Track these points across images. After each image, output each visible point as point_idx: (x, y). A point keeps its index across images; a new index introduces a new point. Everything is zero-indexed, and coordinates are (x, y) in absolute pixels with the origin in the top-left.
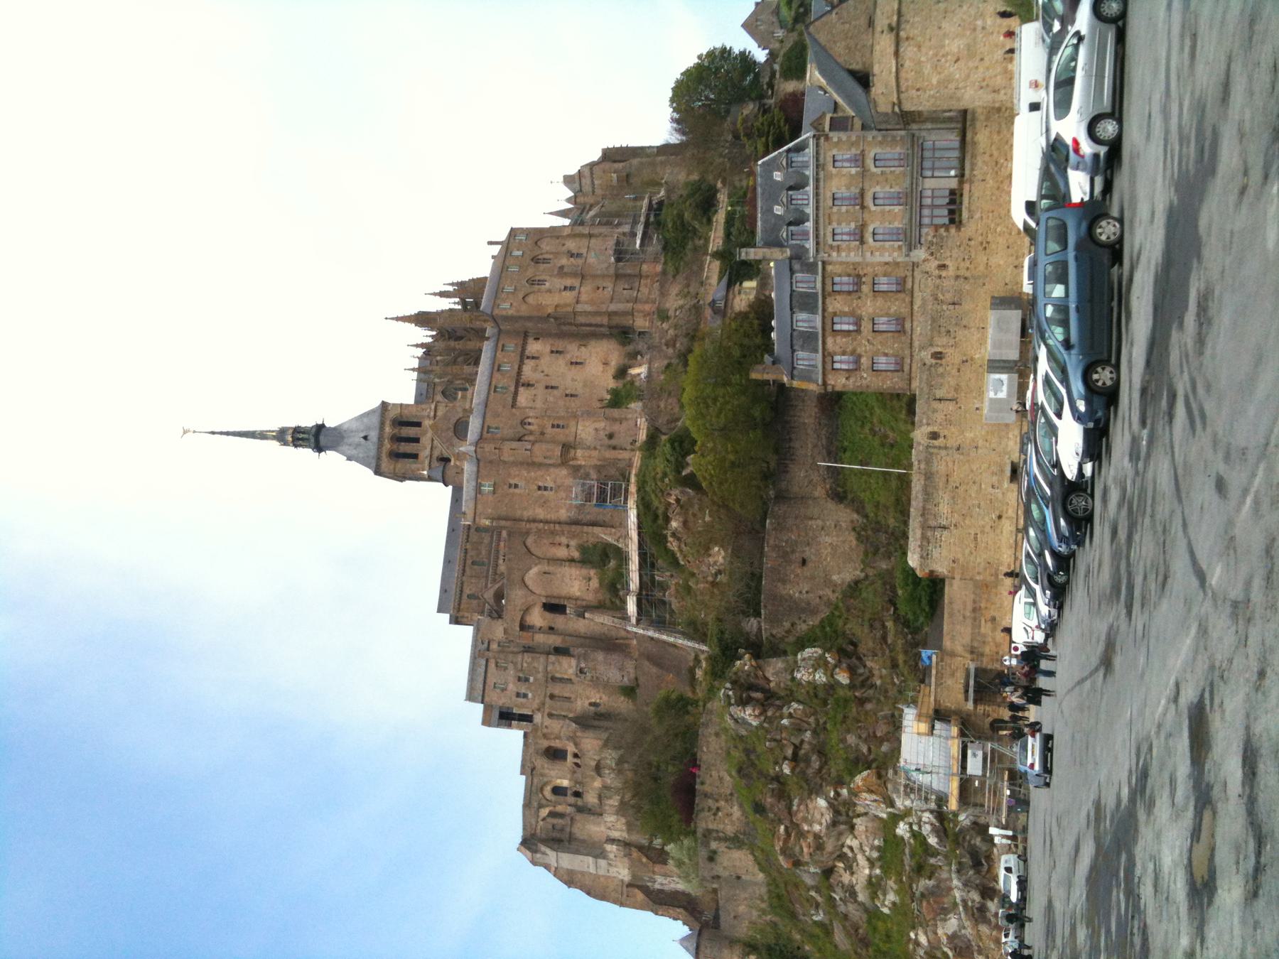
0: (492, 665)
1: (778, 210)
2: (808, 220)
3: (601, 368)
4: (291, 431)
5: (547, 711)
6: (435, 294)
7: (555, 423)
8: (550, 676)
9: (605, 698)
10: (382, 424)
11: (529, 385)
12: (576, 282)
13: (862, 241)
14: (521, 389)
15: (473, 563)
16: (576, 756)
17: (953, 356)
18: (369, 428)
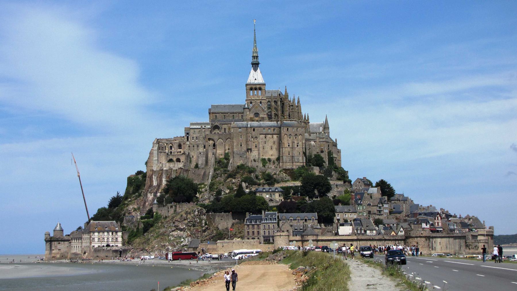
0: (199, 130)
2: (267, 221)
3: (271, 154)
4: (256, 55)
5: (190, 145)
6: (294, 97)
7: (257, 145)
8: (198, 145)
9: (195, 159)
10: (259, 85)
11: (265, 137)
13: (264, 229)
14: (264, 135)
15: (225, 116)
16: (180, 152)
17: (243, 244)
18: (258, 80)
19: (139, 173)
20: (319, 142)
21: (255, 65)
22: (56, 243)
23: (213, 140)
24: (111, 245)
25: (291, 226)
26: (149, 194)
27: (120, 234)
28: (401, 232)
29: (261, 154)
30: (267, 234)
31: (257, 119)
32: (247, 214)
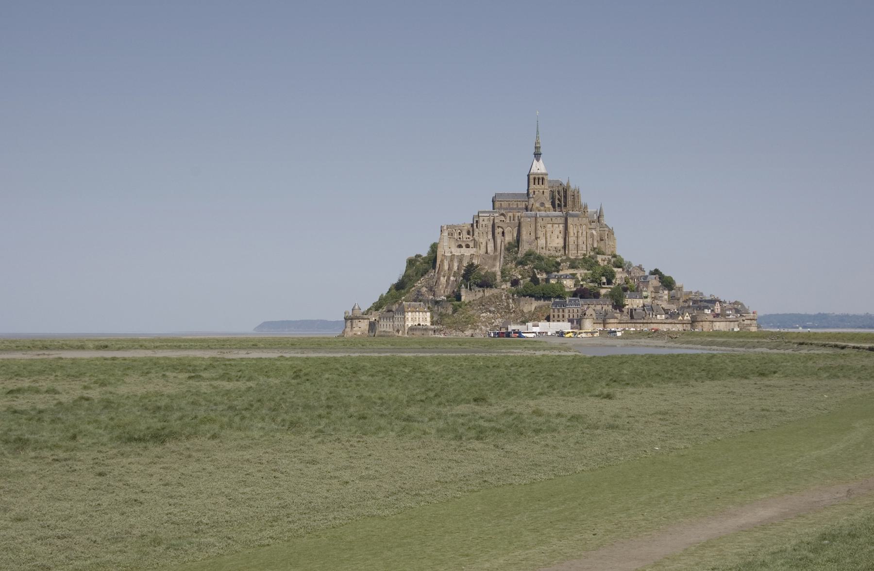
0: (488, 218)
1: (573, 302)
10: (542, 175)
12: (576, 235)
19: (418, 256)
20: (600, 231)
21: (537, 155)
22: (356, 321)
23: (502, 228)
24: (421, 324)
25: (594, 310)
26: (442, 278)
27: (429, 314)
28: (687, 316)
29: (548, 243)
30: (571, 317)
31: (542, 208)
32: (552, 299)
